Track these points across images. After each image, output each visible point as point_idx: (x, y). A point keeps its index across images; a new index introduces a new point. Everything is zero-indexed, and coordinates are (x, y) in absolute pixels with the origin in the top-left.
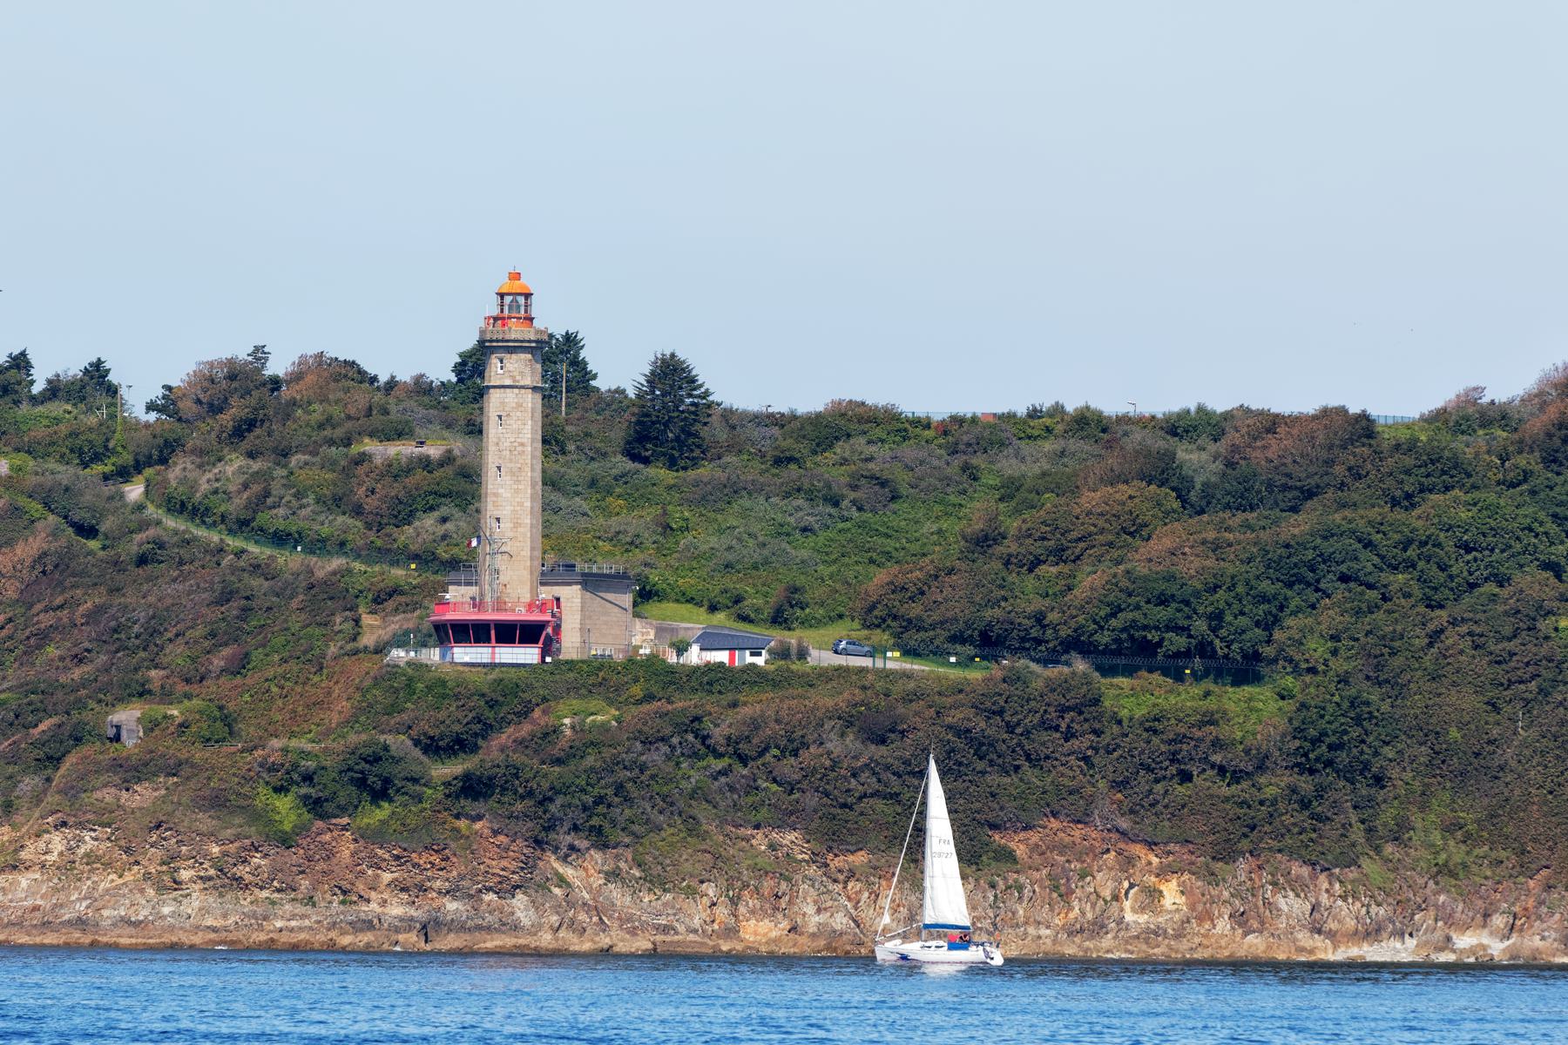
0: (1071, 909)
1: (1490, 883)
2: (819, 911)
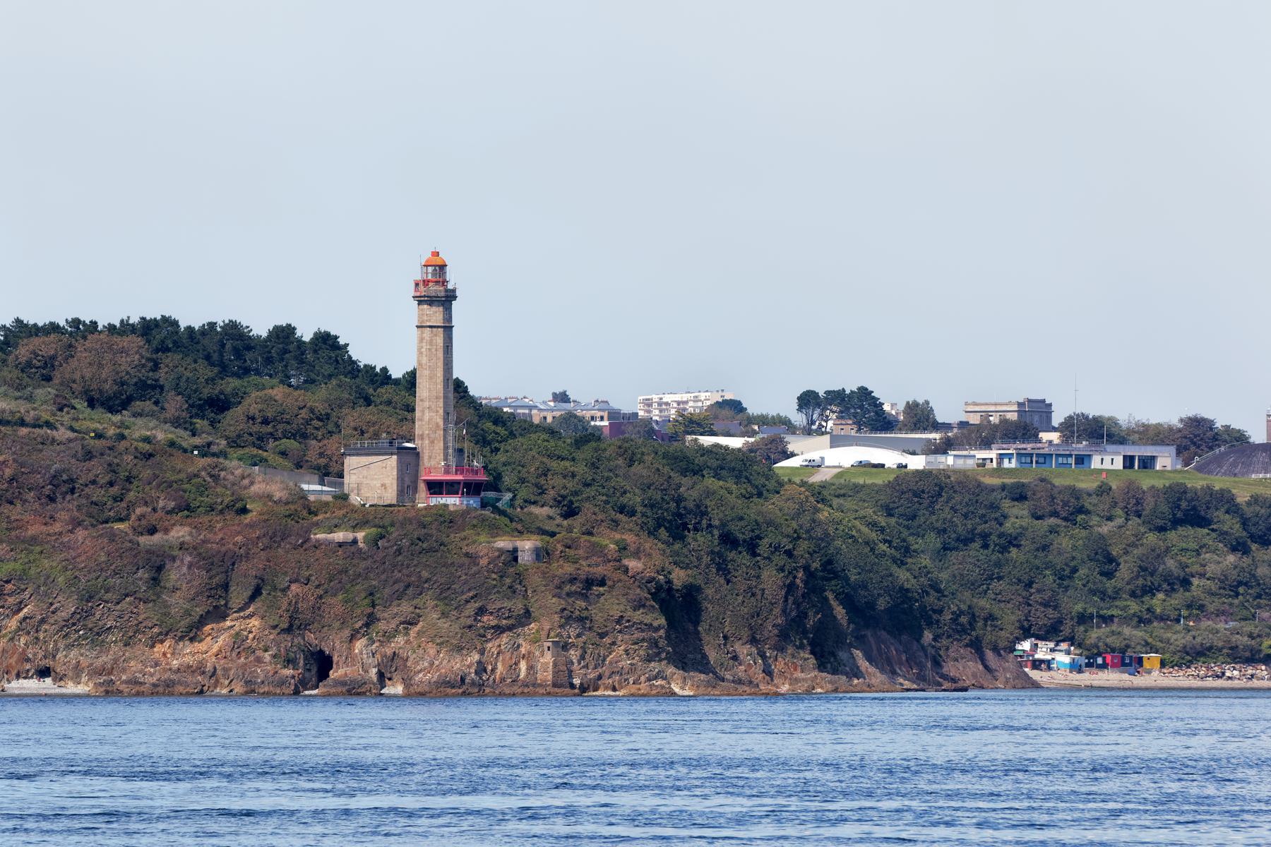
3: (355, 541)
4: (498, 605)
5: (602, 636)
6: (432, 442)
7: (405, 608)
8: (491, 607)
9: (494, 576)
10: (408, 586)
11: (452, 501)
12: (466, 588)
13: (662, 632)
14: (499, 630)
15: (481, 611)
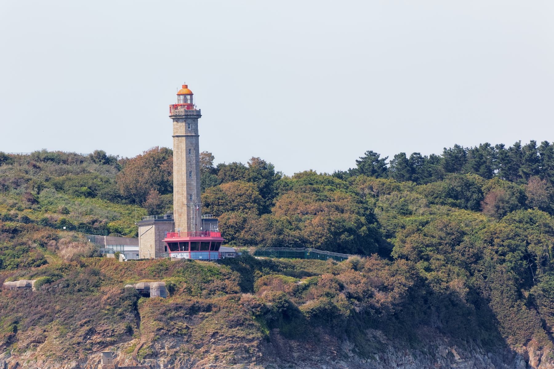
0: (437, 362)
1: (501, 347)
2: (398, 365)
3: (29, 286)
4: (105, 327)
5: (197, 347)
6: (180, 215)
7: (38, 331)
8: (98, 329)
9: (108, 307)
10: (42, 317)
11: (185, 255)
12: (84, 315)
13: (255, 343)
14: (103, 345)
15: (92, 332)
